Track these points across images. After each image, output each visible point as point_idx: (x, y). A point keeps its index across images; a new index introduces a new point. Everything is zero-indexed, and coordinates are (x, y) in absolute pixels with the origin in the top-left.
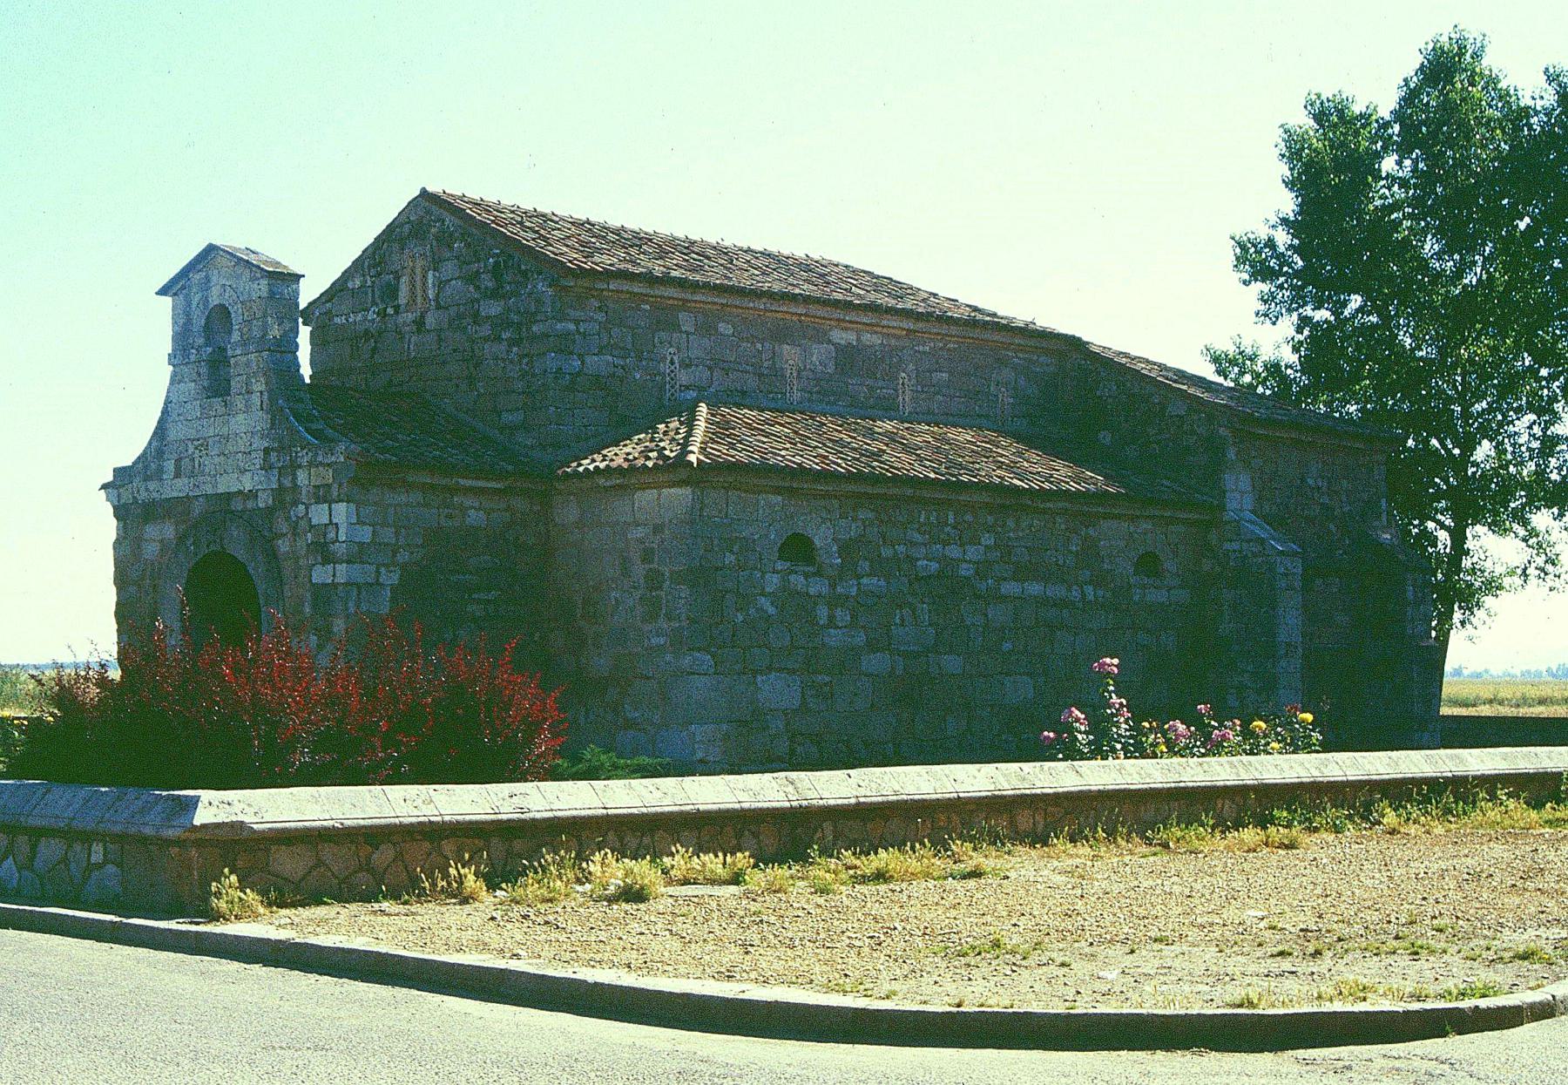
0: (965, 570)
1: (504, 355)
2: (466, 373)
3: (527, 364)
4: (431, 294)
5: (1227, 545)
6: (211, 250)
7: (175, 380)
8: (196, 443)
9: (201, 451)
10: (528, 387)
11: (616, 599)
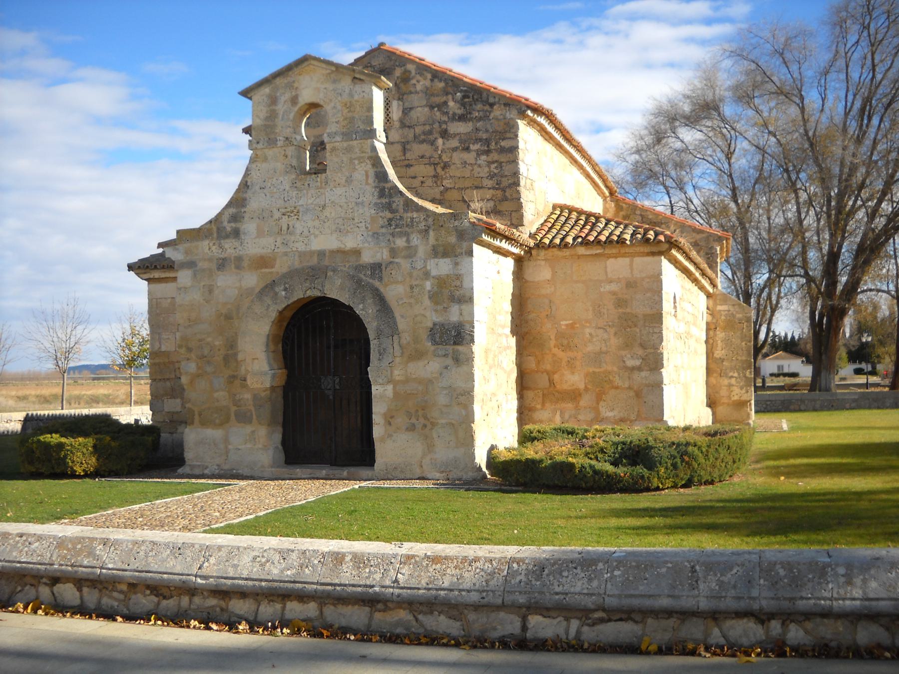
1: (473, 162)
2: (433, 173)
3: (496, 168)
5: (719, 308)
7: (252, 160)
8: (283, 211)
10: (497, 184)
11: (590, 334)
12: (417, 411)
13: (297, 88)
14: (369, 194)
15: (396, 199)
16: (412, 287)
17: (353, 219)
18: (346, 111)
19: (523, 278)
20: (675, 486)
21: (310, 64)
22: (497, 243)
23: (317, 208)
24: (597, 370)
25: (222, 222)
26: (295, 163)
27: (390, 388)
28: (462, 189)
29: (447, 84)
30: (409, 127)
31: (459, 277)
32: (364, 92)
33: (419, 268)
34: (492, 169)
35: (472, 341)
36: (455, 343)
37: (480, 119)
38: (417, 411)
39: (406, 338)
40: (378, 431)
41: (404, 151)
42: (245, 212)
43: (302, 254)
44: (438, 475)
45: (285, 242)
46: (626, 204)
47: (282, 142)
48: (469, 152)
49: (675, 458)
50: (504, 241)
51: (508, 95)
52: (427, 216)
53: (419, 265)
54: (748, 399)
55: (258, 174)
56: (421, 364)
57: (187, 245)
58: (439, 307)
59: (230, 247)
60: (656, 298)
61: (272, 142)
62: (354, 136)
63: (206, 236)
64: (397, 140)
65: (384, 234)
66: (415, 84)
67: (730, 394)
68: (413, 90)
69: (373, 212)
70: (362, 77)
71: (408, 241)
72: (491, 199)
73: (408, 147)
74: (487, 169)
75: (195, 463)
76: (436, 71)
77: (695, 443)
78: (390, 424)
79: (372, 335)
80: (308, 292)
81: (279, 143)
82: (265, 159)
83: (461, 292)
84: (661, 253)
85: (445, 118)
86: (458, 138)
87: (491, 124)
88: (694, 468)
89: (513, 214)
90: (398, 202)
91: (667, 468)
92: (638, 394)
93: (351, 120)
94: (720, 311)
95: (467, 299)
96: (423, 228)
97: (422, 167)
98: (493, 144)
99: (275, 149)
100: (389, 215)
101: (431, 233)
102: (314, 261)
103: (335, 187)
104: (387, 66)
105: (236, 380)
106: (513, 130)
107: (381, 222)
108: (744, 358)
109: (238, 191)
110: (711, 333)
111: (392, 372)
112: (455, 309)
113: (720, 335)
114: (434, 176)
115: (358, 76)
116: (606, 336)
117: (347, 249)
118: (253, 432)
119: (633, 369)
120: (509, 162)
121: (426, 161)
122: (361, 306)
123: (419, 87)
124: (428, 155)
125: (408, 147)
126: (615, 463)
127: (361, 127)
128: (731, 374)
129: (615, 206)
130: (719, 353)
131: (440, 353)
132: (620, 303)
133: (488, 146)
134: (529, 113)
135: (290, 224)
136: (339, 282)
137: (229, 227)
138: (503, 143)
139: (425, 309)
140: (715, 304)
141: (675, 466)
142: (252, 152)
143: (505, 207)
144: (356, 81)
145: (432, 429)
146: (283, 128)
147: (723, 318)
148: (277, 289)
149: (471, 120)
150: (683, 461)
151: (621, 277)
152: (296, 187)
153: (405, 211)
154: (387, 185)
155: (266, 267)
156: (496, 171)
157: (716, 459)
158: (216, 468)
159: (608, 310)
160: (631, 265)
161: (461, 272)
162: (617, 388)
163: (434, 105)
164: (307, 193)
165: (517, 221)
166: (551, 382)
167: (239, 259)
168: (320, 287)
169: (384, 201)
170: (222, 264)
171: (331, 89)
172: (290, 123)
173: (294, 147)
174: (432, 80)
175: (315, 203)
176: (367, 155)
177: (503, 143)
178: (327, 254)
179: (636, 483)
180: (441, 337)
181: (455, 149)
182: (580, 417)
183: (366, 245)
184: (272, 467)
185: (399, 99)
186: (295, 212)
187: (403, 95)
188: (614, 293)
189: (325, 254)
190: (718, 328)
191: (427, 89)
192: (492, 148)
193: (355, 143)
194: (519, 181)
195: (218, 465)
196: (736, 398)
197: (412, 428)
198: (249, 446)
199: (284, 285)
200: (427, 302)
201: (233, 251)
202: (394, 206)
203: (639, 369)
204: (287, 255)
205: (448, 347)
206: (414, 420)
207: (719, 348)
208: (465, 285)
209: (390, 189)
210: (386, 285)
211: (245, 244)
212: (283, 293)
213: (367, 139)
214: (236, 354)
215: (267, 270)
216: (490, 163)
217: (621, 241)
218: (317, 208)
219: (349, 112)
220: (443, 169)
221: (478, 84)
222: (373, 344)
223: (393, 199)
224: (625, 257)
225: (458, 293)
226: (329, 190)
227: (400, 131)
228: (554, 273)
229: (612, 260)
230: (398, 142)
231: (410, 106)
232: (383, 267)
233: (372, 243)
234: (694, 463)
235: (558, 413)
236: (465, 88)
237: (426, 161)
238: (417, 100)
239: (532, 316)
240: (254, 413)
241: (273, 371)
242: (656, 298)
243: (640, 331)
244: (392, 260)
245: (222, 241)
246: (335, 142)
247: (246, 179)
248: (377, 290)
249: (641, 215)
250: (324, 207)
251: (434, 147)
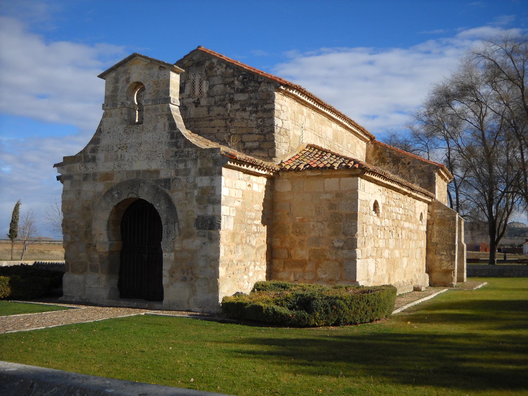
0: (399, 217)
1: (248, 118)
2: (224, 125)
3: (261, 121)
4: (205, 89)
5: (436, 211)
6: (133, 56)
7: (104, 116)
8: (119, 146)
9: (122, 150)
10: (261, 131)
11: (313, 226)
12: (188, 269)
13: (129, 73)
14: (165, 137)
15: (180, 140)
16: (186, 194)
17: (156, 152)
18: (155, 86)
19: (274, 190)
20: (327, 325)
21: (137, 59)
22: (245, 167)
23: (137, 145)
24: (316, 248)
25: (87, 153)
26: (126, 117)
27: (173, 254)
28: (241, 134)
29: (234, 70)
30: (212, 97)
31: (213, 188)
32: (165, 75)
33: (191, 182)
34: (259, 122)
35: (220, 228)
36: (210, 229)
37: (253, 92)
38: (188, 269)
39: (182, 225)
40: (165, 281)
41: (209, 111)
42: (99, 147)
43: (128, 173)
44: (197, 309)
45: (119, 165)
46: (381, 145)
47: (120, 105)
48: (246, 112)
49: (327, 306)
50: (250, 166)
51: (269, 77)
52: (197, 150)
53: (191, 180)
54: (452, 269)
55: (107, 125)
56: (190, 240)
57: (68, 166)
58: (202, 206)
59: (91, 168)
60: (354, 203)
61: (114, 105)
62: (159, 101)
63: (78, 161)
64: (205, 105)
65: (172, 161)
66: (216, 71)
67: (441, 266)
68: (215, 74)
69: (167, 147)
70: (164, 66)
71: (185, 165)
72: (258, 141)
73: (211, 109)
74: (255, 122)
75: (68, 294)
76: (229, 62)
77: (341, 297)
78: (172, 276)
79: (163, 222)
80: (130, 195)
81: (119, 106)
82: (111, 116)
83: (214, 197)
84: (357, 175)
85: (233, 91)
86: (239, 103)
87: (259, 94)
88: (340, 314)
89: (270, 150)
90: (181, 142)
91: (321, 313)
92: (341, 265)
93: (157, 92)
94: (436, 213)
95: (217, 202)
96: (194, 157)
97: (219, 121)
98: (260, 107)
99: (116, 110)
100: (175, 149)
101: (199, 161)
102: (134, 177)
103: (147, 132)
104: (201, 60)
105: (91, 246)
106: (272, 98)
107: (171, 154)
108: (450, 243)
109: (96, 134)
110: (430, 227)
111: (174, 245)
112: (210, 207)
113: (436, 228)
114: (225, 127)
115: (162, 65)
116: (322, 227)
117: (152, 169)
118: (99, 278)
119: (338, 248)
120: (268, 118)
121: (221, 117)
122: (158, 205)
123: (218, 72)
124: (222, 113)
125: (211, 109)
126: (291, 309)
127: (163, 96)
128: (442, 253)
129: (374, 147)
130: (435, 239)
131: (201, 234)
132: (332, 206)
133: (257, 108)
134: (282, 87)
135: (122, 154)
136: (146, 189)
137: (90, 155)
138: (265, 107)
139: (194, 207)
140: (433, 209)
141: (327, 312)
142: (104, 111)
143: (265, 145)
144: (161, 68)
145: (196, 281)
146: (121, 97)
147: (438, 217)
148: (114, 193)
149: (247, 92)
150: (332, 309)
151: (333, 190)
152: (126, 132)
153: (185, 147)
154: (176, 131)
155: (109, 180)
156: (261, 123)
157: (358, 308)
158: (79, 298)
159: (324, 210)
160: (339, 183)
161: (214, 185)
162: (328, 260)
163: (227, 83)
164: (132, 136)
165: (271, 155)
166: (289, 255)
167: (95, 174)
168: (136, 193)
169: (173, 141)
170: (86, 177)
171: (148, 73)
172: (125, 94)
173: (126, 108)
174: (226, 68)
175: (136, 142)
176: (165, 113)
177: (265, 107)
178: (141, 173)
179: (300, 321)
180: (202, 225)
181: (237, 110)
182: (306, 277)
183: (162, 167)
184: (108, 299)
185: (207, 80)
186: (124, 147)
187: (209, 77)
188: (328, 200)
189: (140, 173)
190: (435, 224)
191: (223, 73)
192: (259, 109)
193: (159, 106)
194: (274, 130)
195: (79, 296)
196: (445, 268)
197: (184, 280)
198: (96, 286)
200: (195, 203)
201: (92, 170)
202: (179, 144)
203: (342, 248)
204: (120, 173)
205: (205, 231)
206: (185, 275)
207: (435, 236)
208: (217, 193)
209: (177, 133)
210: (172, 192)
211: (98, 166)
212: (117, 195)
213: (166, 103)
214: (91, 231)
215: (109, 182)
216: (257, 119)
217: (332, 167)
218: (137, 145)
219: (156, 87)
220: (230, 122)
221: (252, 70)
222: (164, 227)
223: (178, 140)
224: (336, 177)
225: (212, 198)
226: (144, 134)
227: (207, 99)
228: (293, 187)
229: (328, 179)
230: (205, 106)
231: (212, 84)
232: (171, 181)
233: (166, 166)
234: (340, 310)
235: (293, 274)
236: (245, 73)
237: (221, 117)
238: (217, 80)
239: (279, 213)
240: (99, 266)
241: (111, 242)
242: (354, 203)
243: (344, 224)
244: (176, 177)
245: (86, 164)
246: (148, 105)
247: (100, 127)
248: (167, 195)
249: (389, 152)
250: (141, 144)
251: (225, 109)
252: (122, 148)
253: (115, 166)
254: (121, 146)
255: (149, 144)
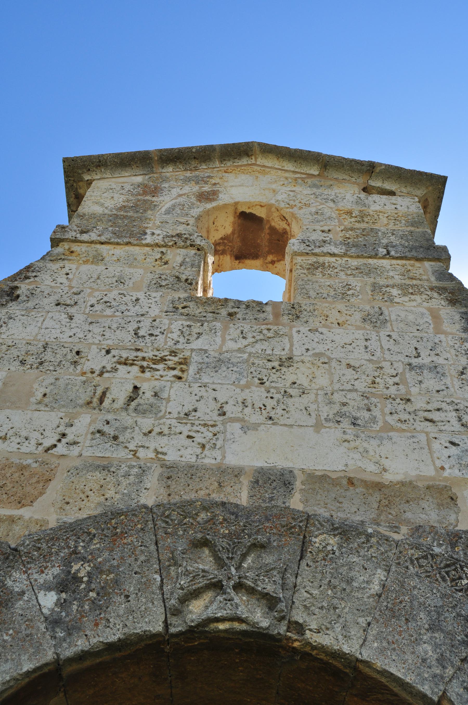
9: (143, 369)
70: (388, 186)
135: (145, 387)
168: (270, 588)
175: (249, 349)
178: (298, 485)
199: (67, 563)
252: (145, 364)
253: (68, 431)
254: (140, 354)
255: (349, 366)
